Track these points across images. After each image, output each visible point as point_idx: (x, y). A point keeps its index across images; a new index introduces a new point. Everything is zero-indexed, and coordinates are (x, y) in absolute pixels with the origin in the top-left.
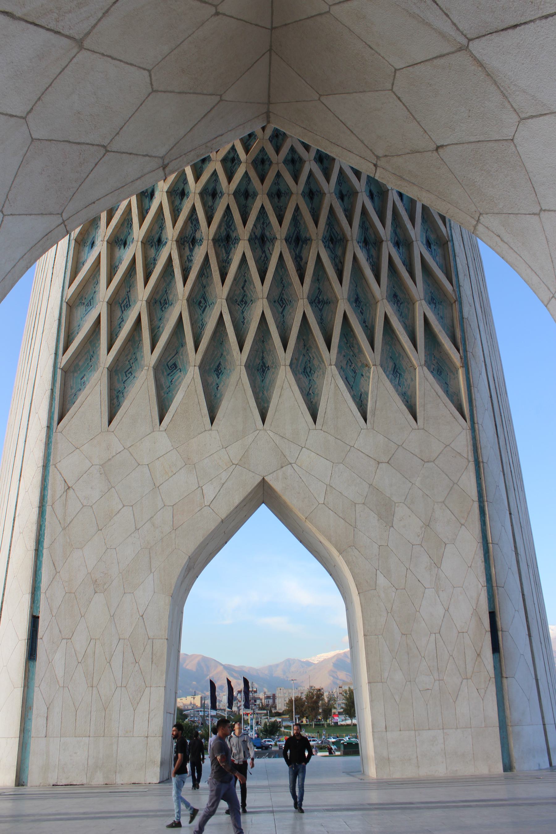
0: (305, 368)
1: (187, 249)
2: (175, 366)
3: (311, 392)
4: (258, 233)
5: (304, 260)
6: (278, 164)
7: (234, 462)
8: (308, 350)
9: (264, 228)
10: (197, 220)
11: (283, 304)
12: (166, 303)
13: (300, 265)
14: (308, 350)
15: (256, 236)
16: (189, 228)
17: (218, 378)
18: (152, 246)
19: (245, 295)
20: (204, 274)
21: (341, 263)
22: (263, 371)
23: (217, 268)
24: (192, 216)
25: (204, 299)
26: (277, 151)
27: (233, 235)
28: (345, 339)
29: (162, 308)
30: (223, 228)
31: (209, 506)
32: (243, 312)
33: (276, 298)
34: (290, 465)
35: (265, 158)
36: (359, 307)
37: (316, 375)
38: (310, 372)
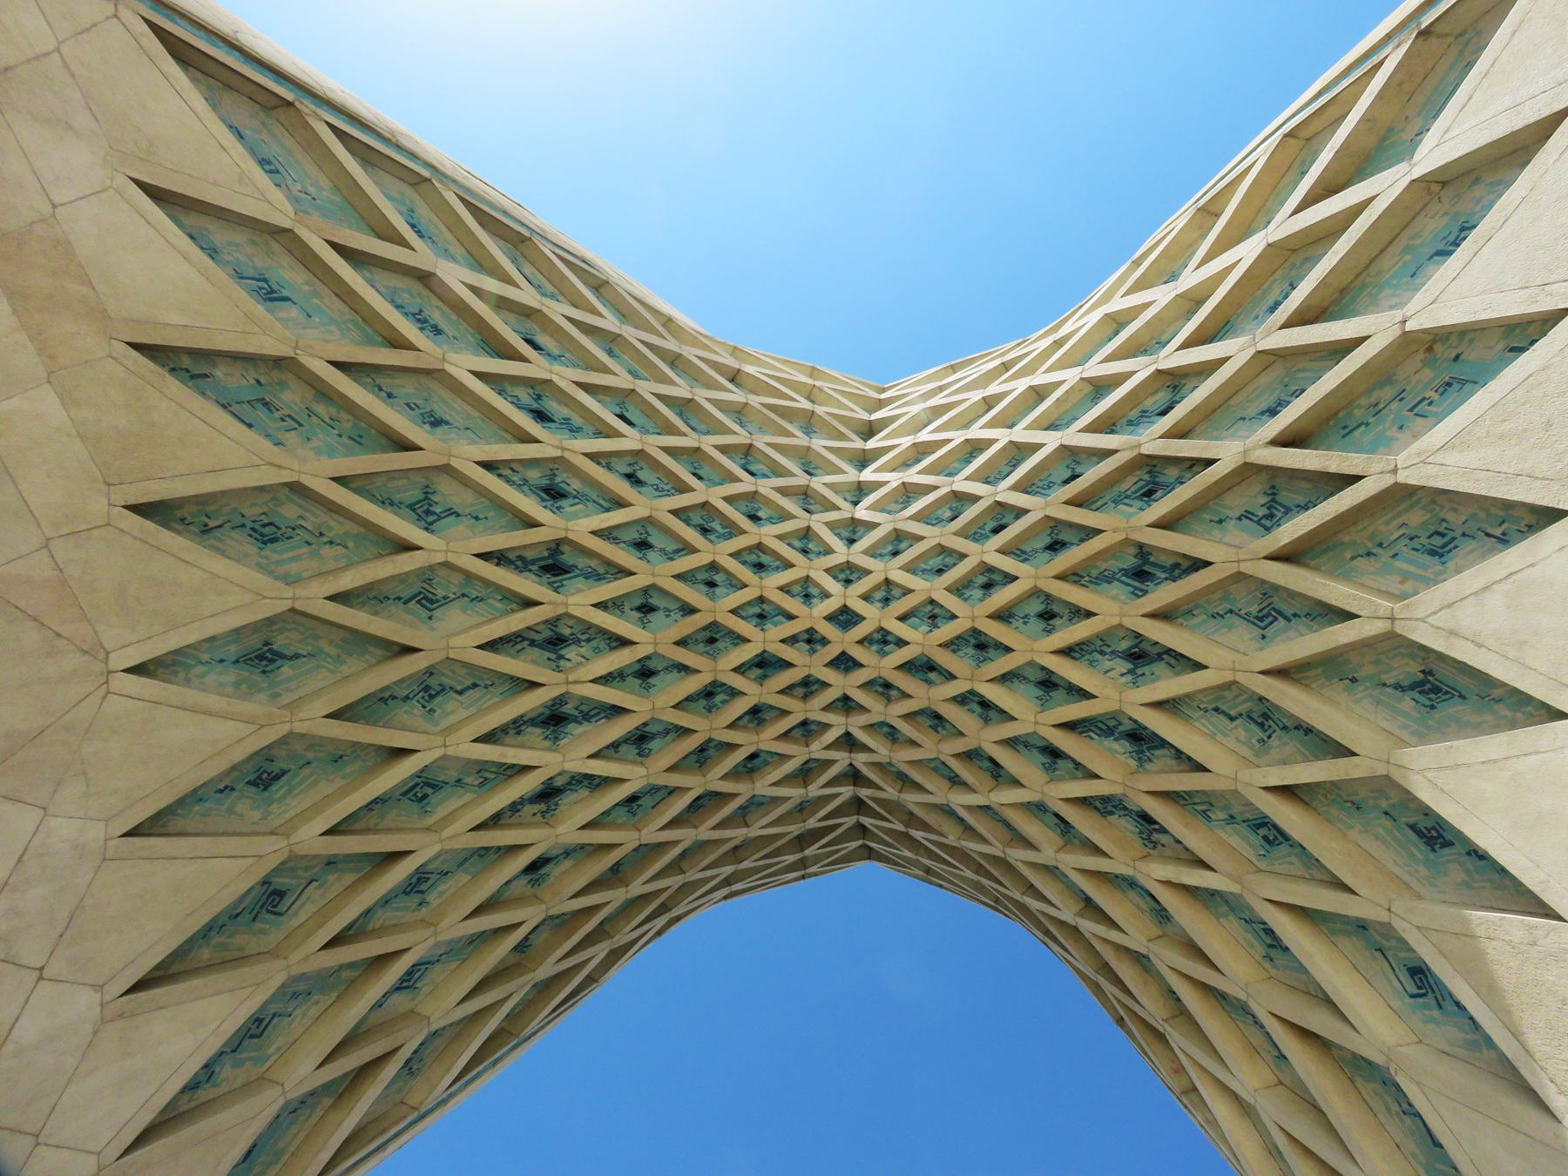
0: (1432, 553)
1: (1163, 838)
3: (1498, 532)
4: (1122, 666)
5: (1180, 560)
6: (973, 619)
8: (1380, 545)
9: (1113, 652)
10: (1106, 800)
11: (1269, 615)
15: (1130, 672)
16: (1122, 821)
17: (1451, 844)
21: (1191, 467)
23: (1174, 777)
24: (1097, 809)
25: (1259, 826)
26: (954, 617)
27: (1127, 726)
28: (1357, 433)
30: (1115, 745)
32: (1284, 728)
33: (1257, 632)
35: (973, 641)
37: (1450, 516)
38: (1443, 535)
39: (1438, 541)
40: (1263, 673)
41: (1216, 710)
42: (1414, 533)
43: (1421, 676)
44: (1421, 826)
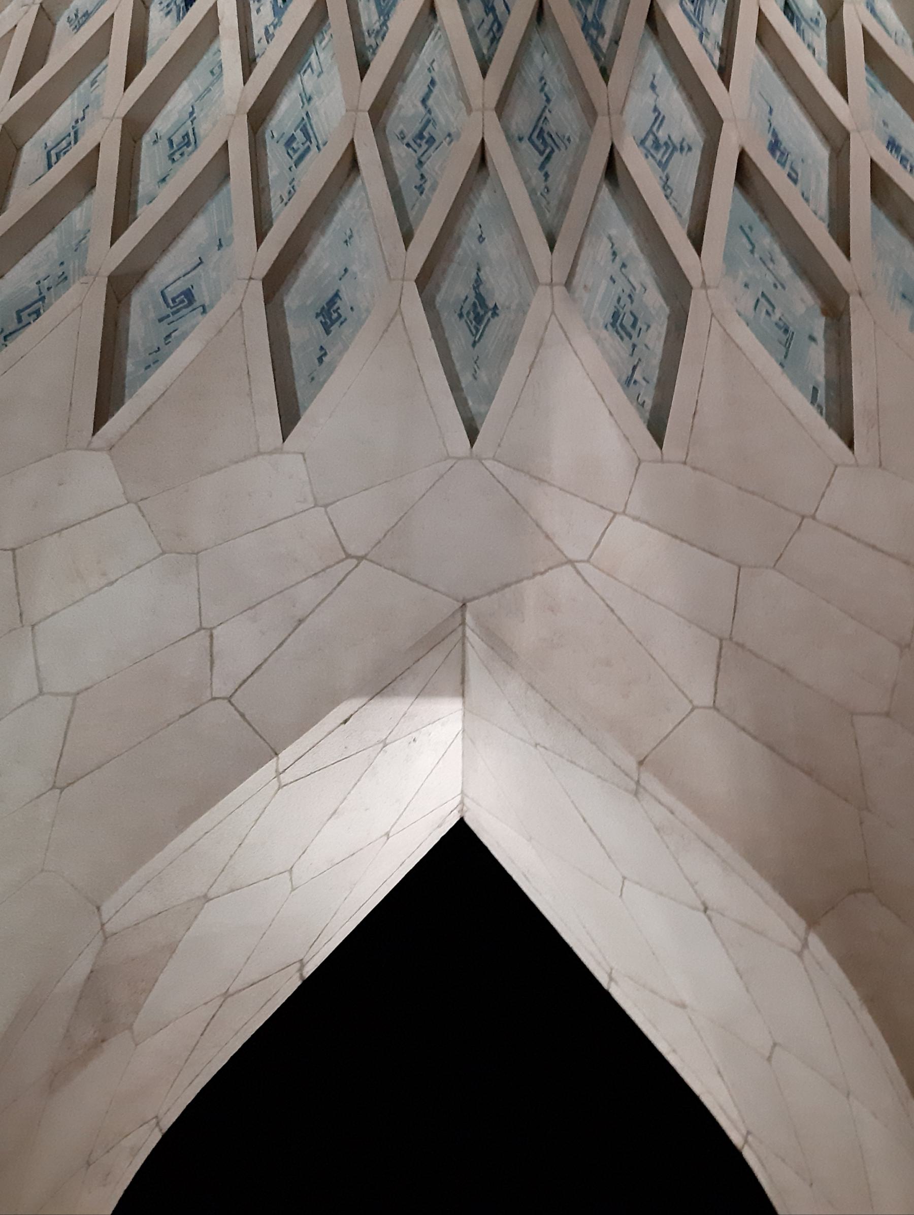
0: (615, 316)
2: (189, 295)
7: (352, 549)
8: (624, 265)
12: (188, 144)
13: (599, 47)
14: (624, 265)
17: (328, 332)
18: (168, 13)
19: (428, 121)
20: (310, 65)
22: (478, 319)
28: (745, 240)
29: (173, 154)
31: (229, 699)
32: (421, 163)
33: (526, 130)
34: (569, 567)
36: (783, 165)
38: (634, 325)
39: (628, 321)
40: (483, 141)
41: (433, 82)
42: (635, 298)
43: (491, 305)
44: (339, 303)
